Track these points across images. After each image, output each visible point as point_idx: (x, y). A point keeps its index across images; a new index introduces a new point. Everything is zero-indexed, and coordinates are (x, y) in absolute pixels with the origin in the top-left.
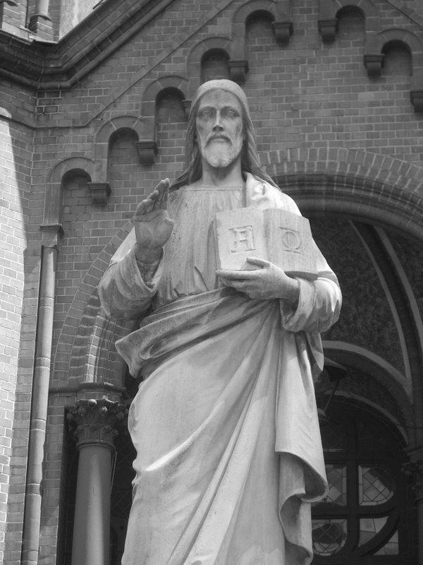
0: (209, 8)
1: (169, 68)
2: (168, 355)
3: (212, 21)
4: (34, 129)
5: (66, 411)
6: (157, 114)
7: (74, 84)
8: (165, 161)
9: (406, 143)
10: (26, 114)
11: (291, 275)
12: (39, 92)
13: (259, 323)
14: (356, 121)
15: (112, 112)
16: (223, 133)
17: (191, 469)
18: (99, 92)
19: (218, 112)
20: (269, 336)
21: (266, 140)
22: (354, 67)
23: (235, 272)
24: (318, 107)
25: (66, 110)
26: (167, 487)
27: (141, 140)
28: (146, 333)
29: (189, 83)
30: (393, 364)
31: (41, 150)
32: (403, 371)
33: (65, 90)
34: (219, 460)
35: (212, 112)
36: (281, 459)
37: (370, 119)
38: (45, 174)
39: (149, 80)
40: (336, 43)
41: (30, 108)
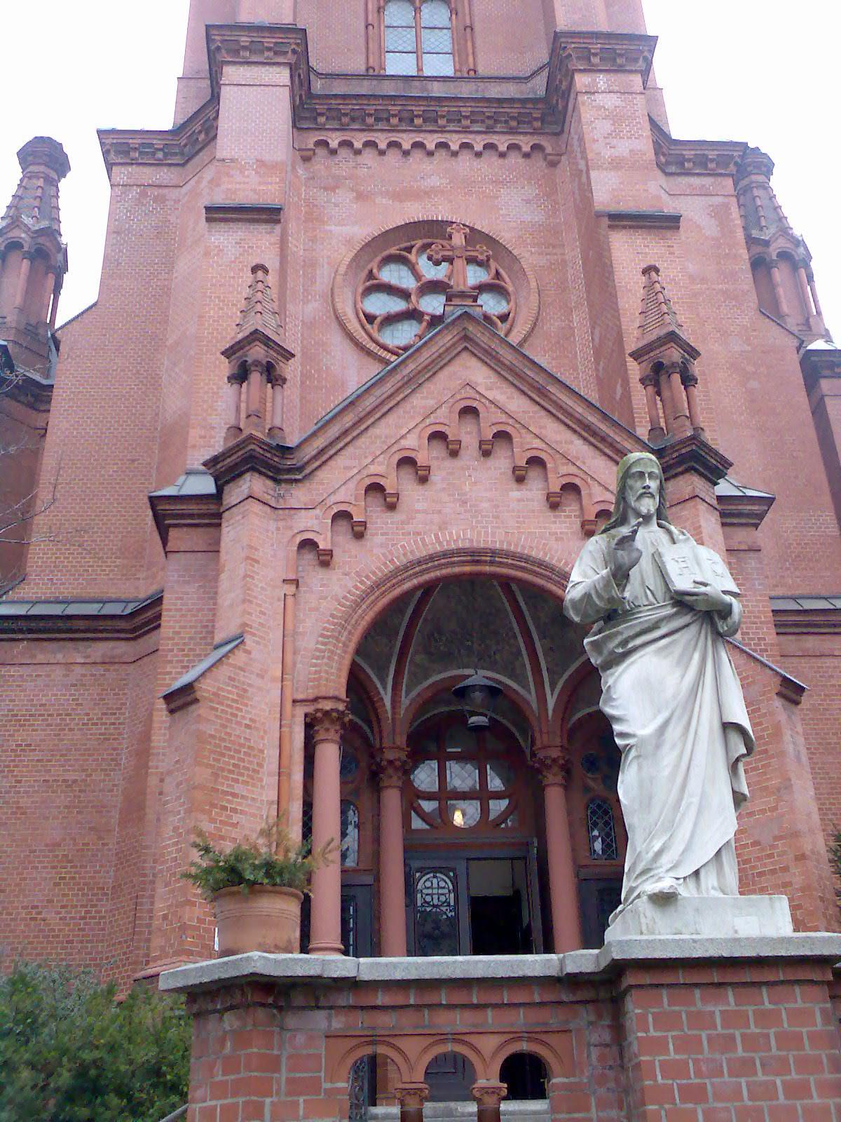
0: (401, 427)
1: (373, 469)
2: (635, 649)
3: (403, 437)
4: (276, 508)
5: (306, 715)
6: (365, 502)
7: (305, 477)
8: (373, 535)
9: (545, 528)
10: (269, 497)
11: (725, 592)
13: (698, 627)
14: (508, 511)
15: (333, 499)
16: (650, 490)
17: (674, 733)
18: (323, 484)
19: (647, 475)
20: (706, 638)
21: (445, 523)
22: (504, 473)
23: (689, 590)
25: (298, 495)
26: (658, 746)
27: (355, 520)
28: (618, 633)
29: (388, 481)
30: (523, 687)
31: (281, 524)
33: (296, 481)
34: (689, 723)
35: (642, 474)
36: (728, 727)
37: (519, 511)
38: (285, 540)
39: (358, 477)
40: (492, 456)
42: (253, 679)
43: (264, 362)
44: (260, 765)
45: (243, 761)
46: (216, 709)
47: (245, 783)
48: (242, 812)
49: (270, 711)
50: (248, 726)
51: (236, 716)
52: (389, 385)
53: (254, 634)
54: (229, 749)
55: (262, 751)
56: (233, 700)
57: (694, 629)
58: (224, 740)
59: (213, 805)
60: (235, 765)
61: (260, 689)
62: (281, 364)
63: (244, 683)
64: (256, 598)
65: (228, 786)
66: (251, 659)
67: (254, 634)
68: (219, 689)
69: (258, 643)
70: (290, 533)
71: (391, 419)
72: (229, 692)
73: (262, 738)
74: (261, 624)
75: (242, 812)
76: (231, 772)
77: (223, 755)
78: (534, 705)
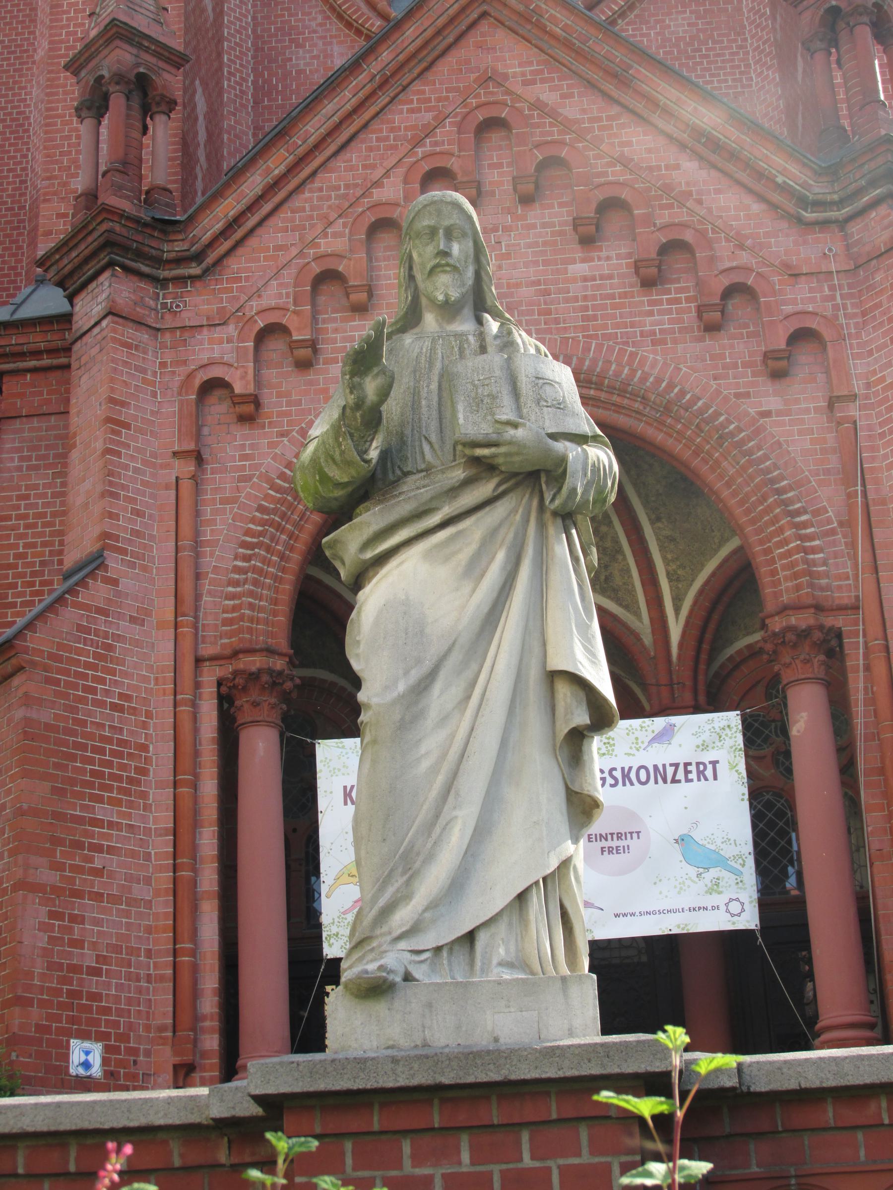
0: (373, 167)
1: (326, 245)
3: (378, 184)
4: (158, 330)
5: (220, 684)
6: (314, 304)
7: (206, 271)
9: (633, 324)
11: (554, 436)
12: (162, 283)
14: (566, 300)
16: (451, 261)
18: (239, 279)
22: (561, 233)
24: (518, 285)
27: (294, 338)
29: (352, 263)
30: (626, 607)
32: (637, 614)
33: (193, 278)
34: (473, 684)
37: (585, 298)
40: (537, 205)
41: (152, 303)
42: (124, 627)
43: (132, 76)
44: (144, 772)
45: (109, 764)
46: (57, 682)
47: (117, 802)
48: (111, 850)
49: (156, 679)
50: (115, 707)
51: (93, 691)
52: (347, 94)
53: (124, 552)
54: (84, 747)
55: (144, 748)
56: (87, 665)
57: (500, 510)
58: (74, 733)
59: (57, 841)
60: (93, 773)
61: (137, 643)
62: (166, 76)
63: (106, 635)
64: (124, 487)
65: (84, 808)
66: (118, 594)
67: (124, 552)
68: (60, 646)
69: (132, 565)
70: (183, 371)
71: (353, 156)
72: (79, 651)
73: (145, 725)
74: (136, 533)
75: (111, 850)
76: (91, 785)
77: (73, 758)
78: (647, 639)
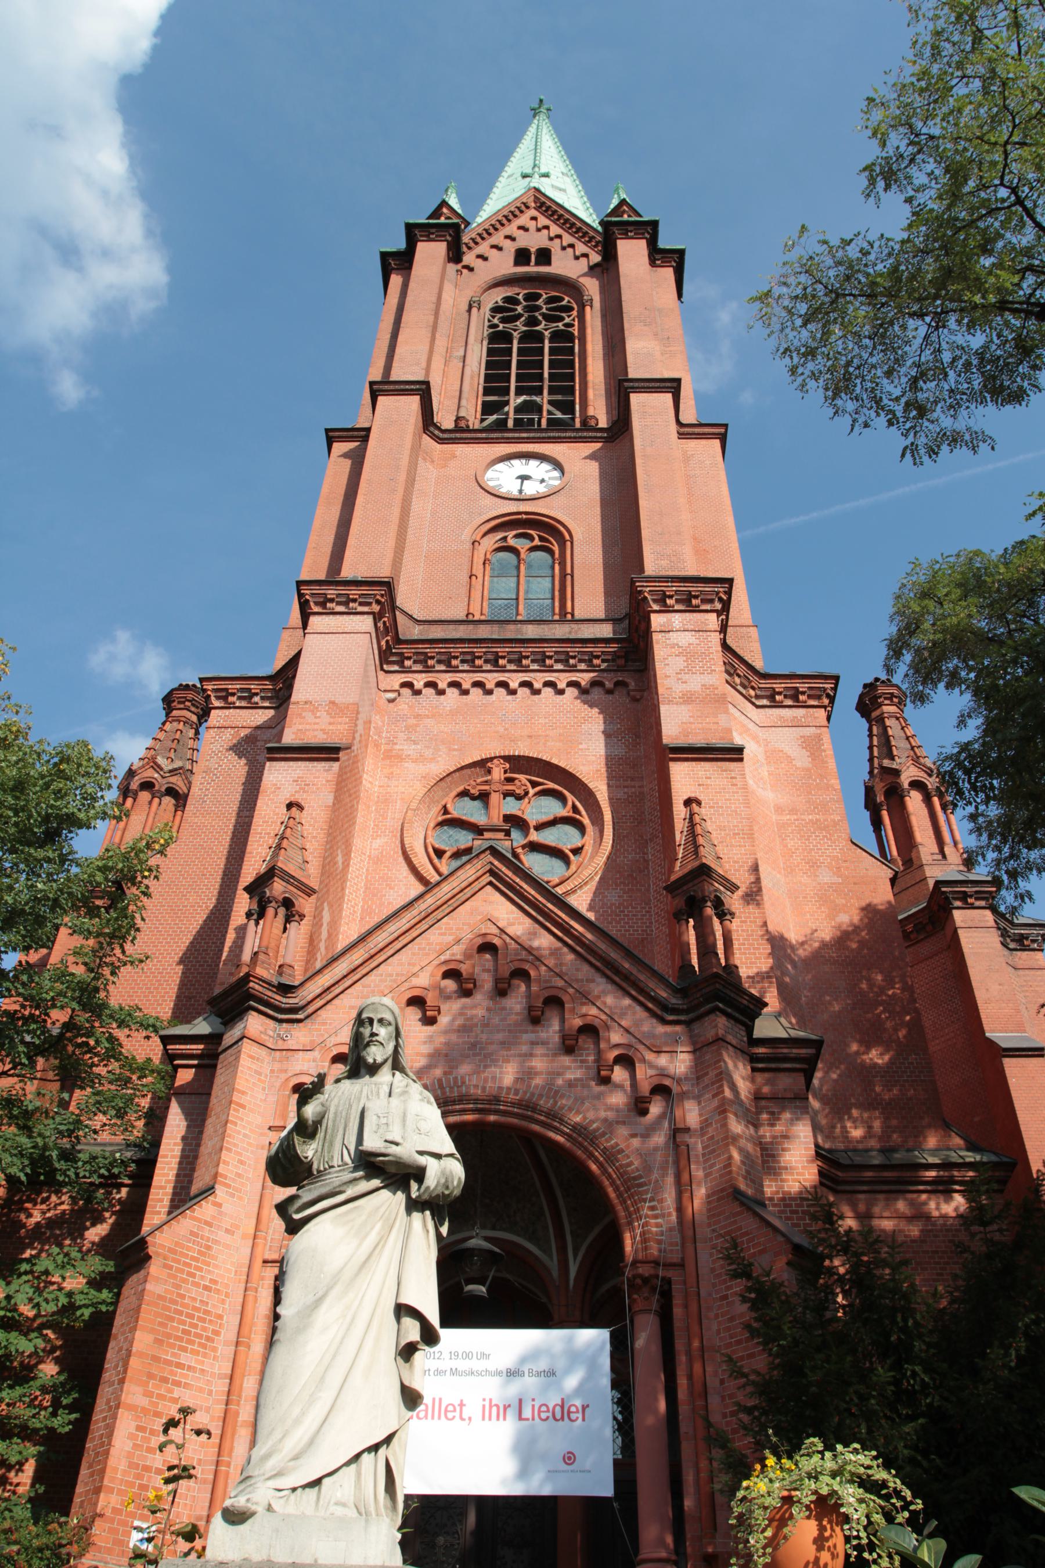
10: (267, 1038)
11: (421, 1153)
12: (281, 1021)
18: (324, 1024)
24: (492, 1043)
25: (298, 1035)
30: (544, 1251)
32: (551, 1257)
36: (403, 1310)
38: (278, 1084)
41: (271, 1033)
42: (221, 1236)
43: (280, 898)
44: (217, 1333)
45: (195, 1326)
46: (170, 1268)
47: (197, 1353)
48: (186, 1386)
49: (236, 1272)
50: (206, 1288)
51: (193, 1275)
52: (404, 921)
53: (228, 1186)
54: (180, 1313)
55: (220, 1317)
56: (193, 1258)
58: (175, 1303)
59: (151, 1376)
60: (184, 1332)
61: (228, 1247)
62: (301, 899)
63: (208, 1239)
64: (235, 1145)
65: (174, 1355)
66: (221, 1213)
67: (228, 1186)
68: (177, 1244)
69: (233, 1195)
70: (284, 1076)
71: (403, 956)
72: (189, 1249)
73: (223, 1302)
74: (239, 1175)
75: (186, 1386)
76: (181, 1339)
77: (172, 1319)
78: (555, 1273)
